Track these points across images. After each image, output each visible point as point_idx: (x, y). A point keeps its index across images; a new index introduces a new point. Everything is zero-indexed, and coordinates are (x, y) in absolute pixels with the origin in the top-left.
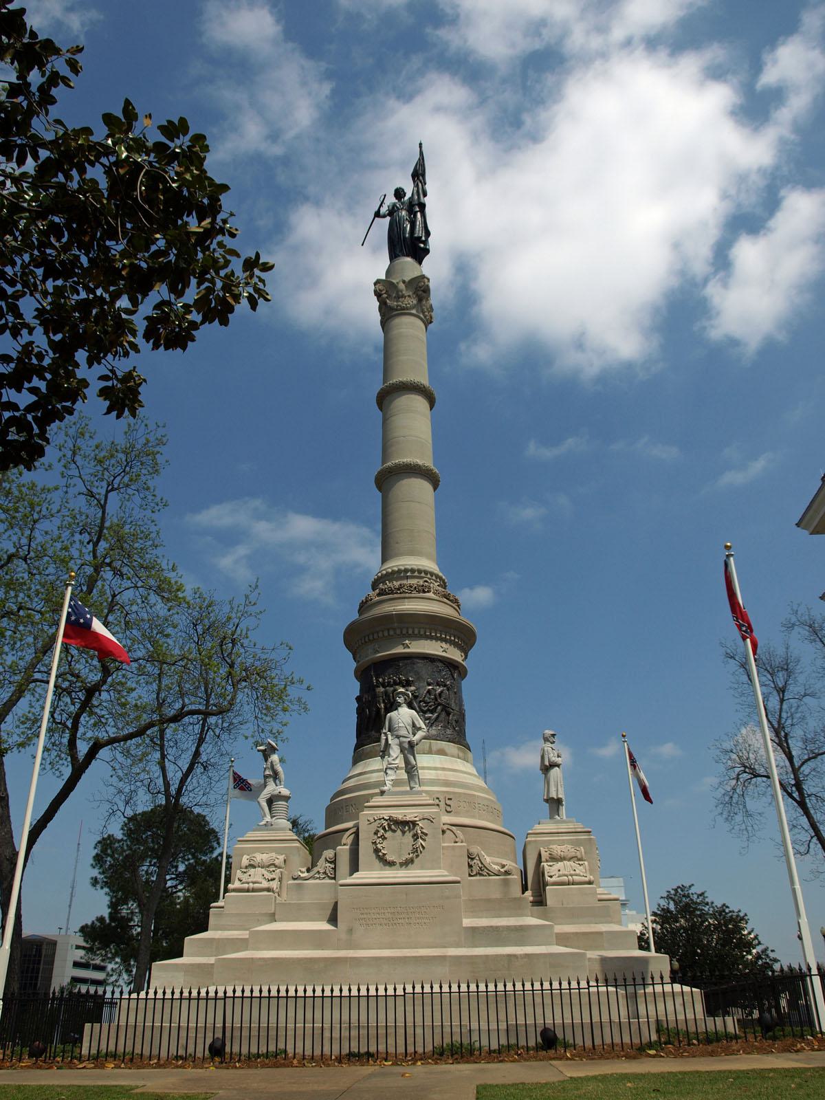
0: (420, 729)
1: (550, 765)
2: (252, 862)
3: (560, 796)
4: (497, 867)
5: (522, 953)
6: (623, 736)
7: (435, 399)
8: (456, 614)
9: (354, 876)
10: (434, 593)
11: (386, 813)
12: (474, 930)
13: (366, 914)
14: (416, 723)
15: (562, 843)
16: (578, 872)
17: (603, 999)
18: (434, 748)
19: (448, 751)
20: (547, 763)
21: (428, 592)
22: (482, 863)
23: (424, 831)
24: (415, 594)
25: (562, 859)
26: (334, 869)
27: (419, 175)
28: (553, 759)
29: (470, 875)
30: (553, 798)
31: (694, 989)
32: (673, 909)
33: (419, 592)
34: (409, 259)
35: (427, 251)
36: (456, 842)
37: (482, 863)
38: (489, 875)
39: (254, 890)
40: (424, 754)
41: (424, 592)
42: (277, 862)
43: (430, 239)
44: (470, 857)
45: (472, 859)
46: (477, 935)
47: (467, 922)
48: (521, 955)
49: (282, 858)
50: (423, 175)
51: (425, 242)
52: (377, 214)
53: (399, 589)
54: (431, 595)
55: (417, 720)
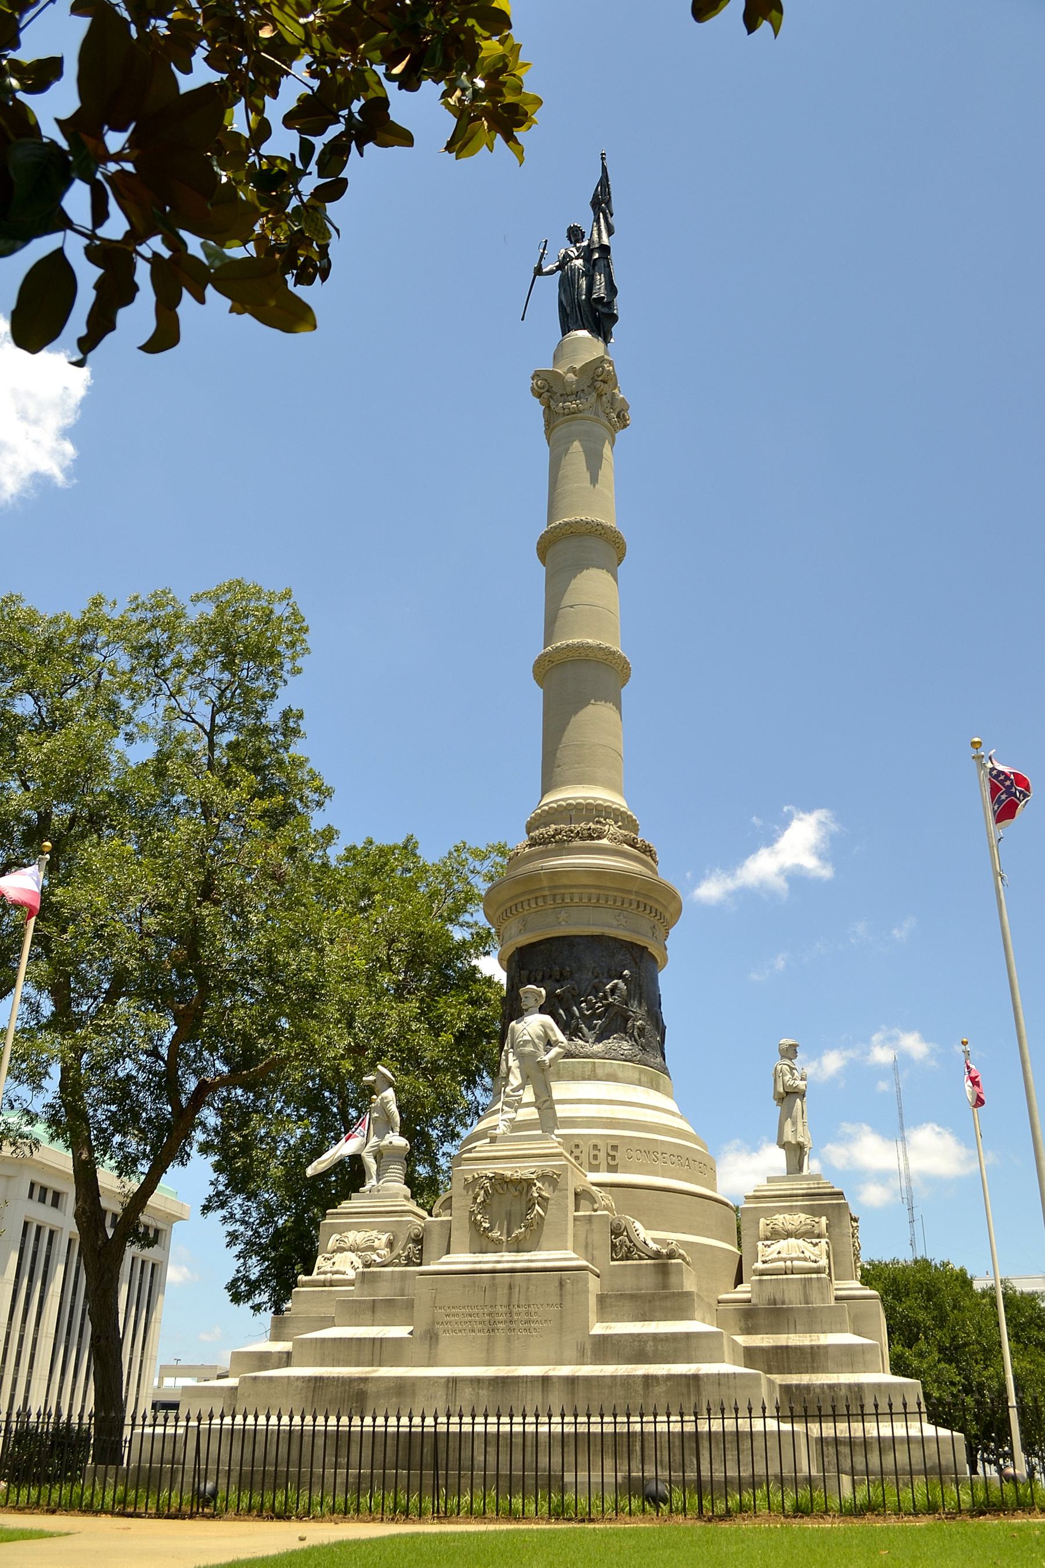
0: (556, 1043)
1: (787, 1093)
2: (342, 1245)
3: (801, 1140)
4: (654, 1246)
5: (665, 1373)
6: (964, 1043)
7: (624, 543)
8: (649, 873)
9: (441, 1260)
10: (610, 839)
11: (490, 1169)
12: (604, 1339)
13: (453, 1315)
14: (551, 1033)
15: (790, 1210)
16: (807, 1254)
17: (787, 1442)
18: (600, 1072)
19: (620, 1075)
20: (781, 1090)
21: (599, 838)
22: (631, 1241)
23: (543, 1193)
24: (578, 843)
25: (789, 1235)
26: (421, 1251)
27: (601, 203)
28: (791, 1082)
29: (613, 1259)
30: (790, 1143)
31: (955, 1433)
32: (267, 1294)
33: (582, 839)
34: (584, 333)
35: (614, 318)
36: (595, 1211)
37: (631, 1241)
38: (641, 1258)
39: (332, 1283)
40: (584, 1079)
41: (593, 839)
42: (376, 1244)
43: (617, 300)
44: (616, 1232)
45: (618, 1235)
46: (605, 1348)
47: (598, 1329)
48: (662, 1376)
49: (384, 1238)
50: (608, 203)
51: (610, 304)
52: (539, 271)
53: (553, 836)
54: (605, 841)
55: (552, 1030)
